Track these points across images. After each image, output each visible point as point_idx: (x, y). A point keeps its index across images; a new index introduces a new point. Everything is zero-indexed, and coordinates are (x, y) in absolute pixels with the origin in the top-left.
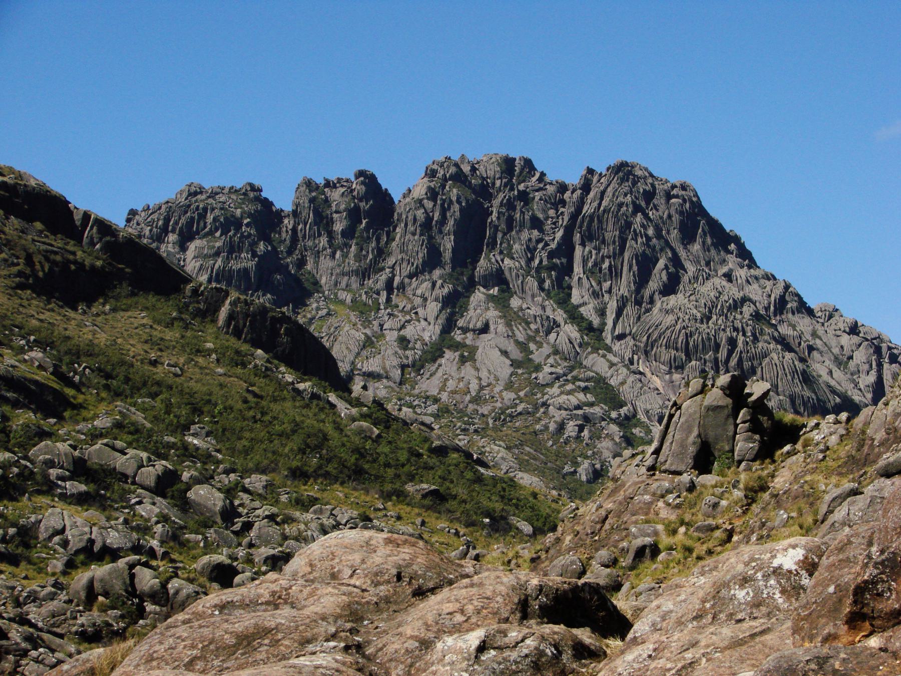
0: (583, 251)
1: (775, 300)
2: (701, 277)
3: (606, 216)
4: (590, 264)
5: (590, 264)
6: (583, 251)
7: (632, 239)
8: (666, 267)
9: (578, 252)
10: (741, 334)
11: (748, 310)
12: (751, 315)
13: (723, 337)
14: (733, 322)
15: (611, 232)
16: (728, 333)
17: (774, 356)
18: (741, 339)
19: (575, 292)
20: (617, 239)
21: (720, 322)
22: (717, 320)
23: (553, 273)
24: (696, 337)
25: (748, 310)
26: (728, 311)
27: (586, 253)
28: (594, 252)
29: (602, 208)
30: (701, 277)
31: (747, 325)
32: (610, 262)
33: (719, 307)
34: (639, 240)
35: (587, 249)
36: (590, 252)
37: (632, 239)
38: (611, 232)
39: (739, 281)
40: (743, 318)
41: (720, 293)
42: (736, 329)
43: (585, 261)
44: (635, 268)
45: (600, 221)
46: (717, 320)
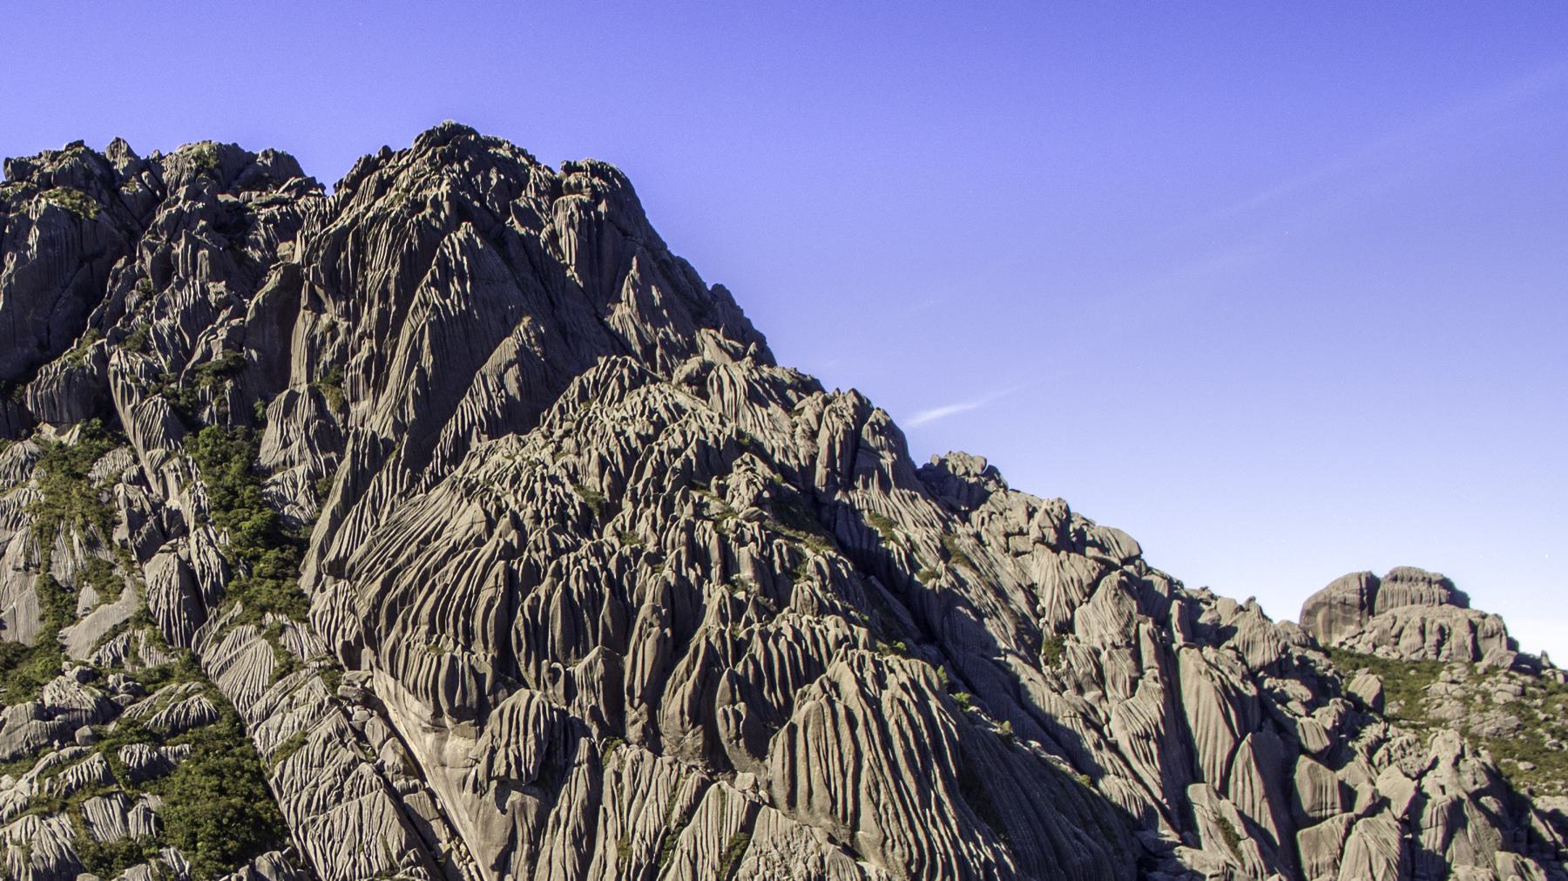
0: (315, 324)
1: (831, 447)
2: (614, 383)
3: (374, 230)
4: (327, 357)
5: (327, 357)
6: (315, 324)
7: (434, 283)
8: (523, 353)
9: (303, 324)
10: (715, 572)
11: (742, 484)
12: (758, 501)
13: (649, 586)
14: (689, 528)
15: (380, 269)
16: (668, 573)
17: (839, 670)
18: (714, 595)
19: (271, 434)
20: (392, 286)
21: (643, 527)
22: (635, 519)
23: (228, 384)
24: (542, 590)
25: (742, 484)
26: (675, 488)
27: (318, 331)
28: (343, 325)
29: (371, 214)
30: (614, 383)
31: (741, 541)
32: (371, 348)
33: (648, 473)
34: (454, 287)
35: (325, 319)
36: (333, 327)
37: (434, 283)
38: (380, 269)
39: (729, 395)
40: (729, 511)
41: (660, 426)
42: (697, 554)
43: (314, 352)
44: (427, 360)
45: (360, 247)
46: (635, 519)
